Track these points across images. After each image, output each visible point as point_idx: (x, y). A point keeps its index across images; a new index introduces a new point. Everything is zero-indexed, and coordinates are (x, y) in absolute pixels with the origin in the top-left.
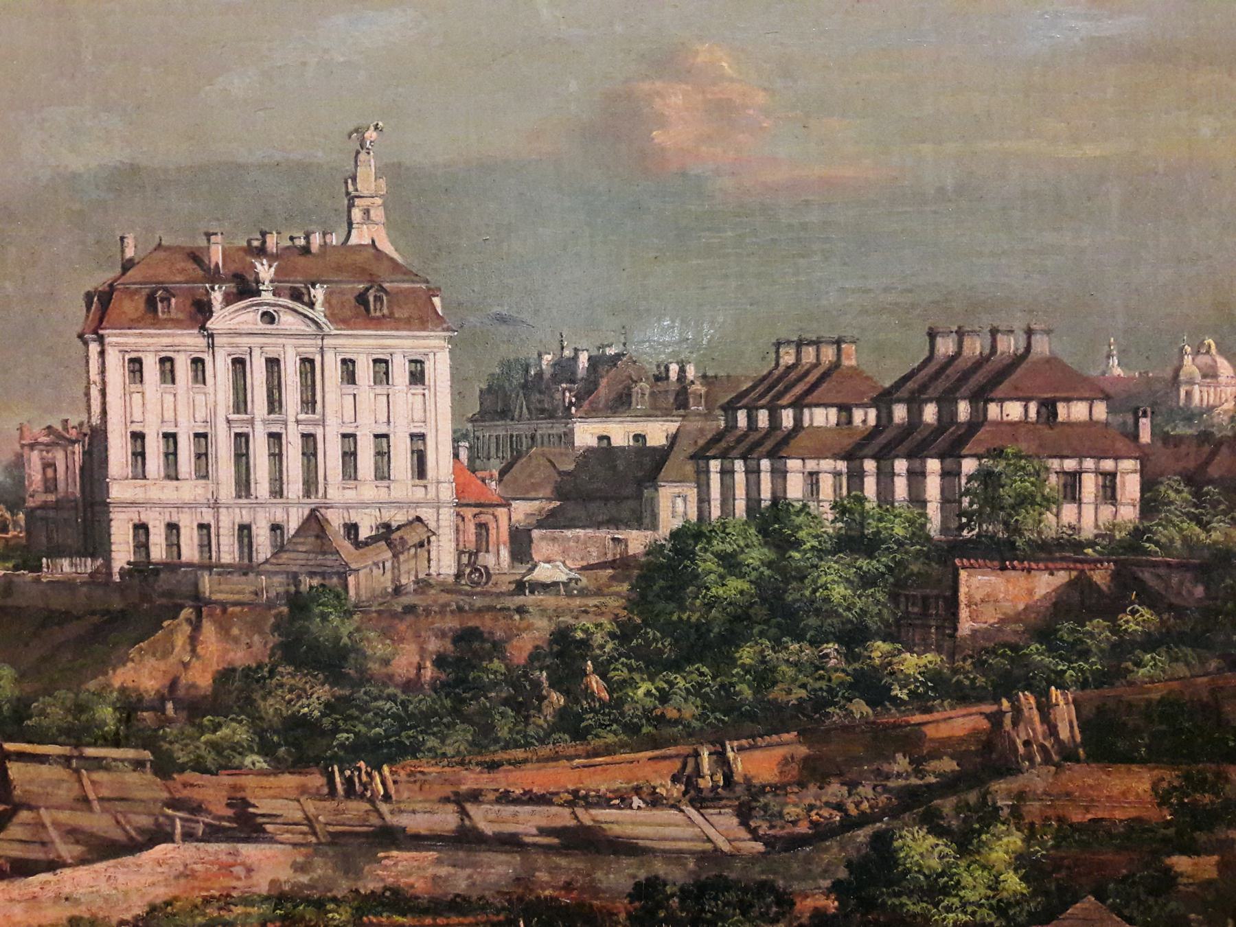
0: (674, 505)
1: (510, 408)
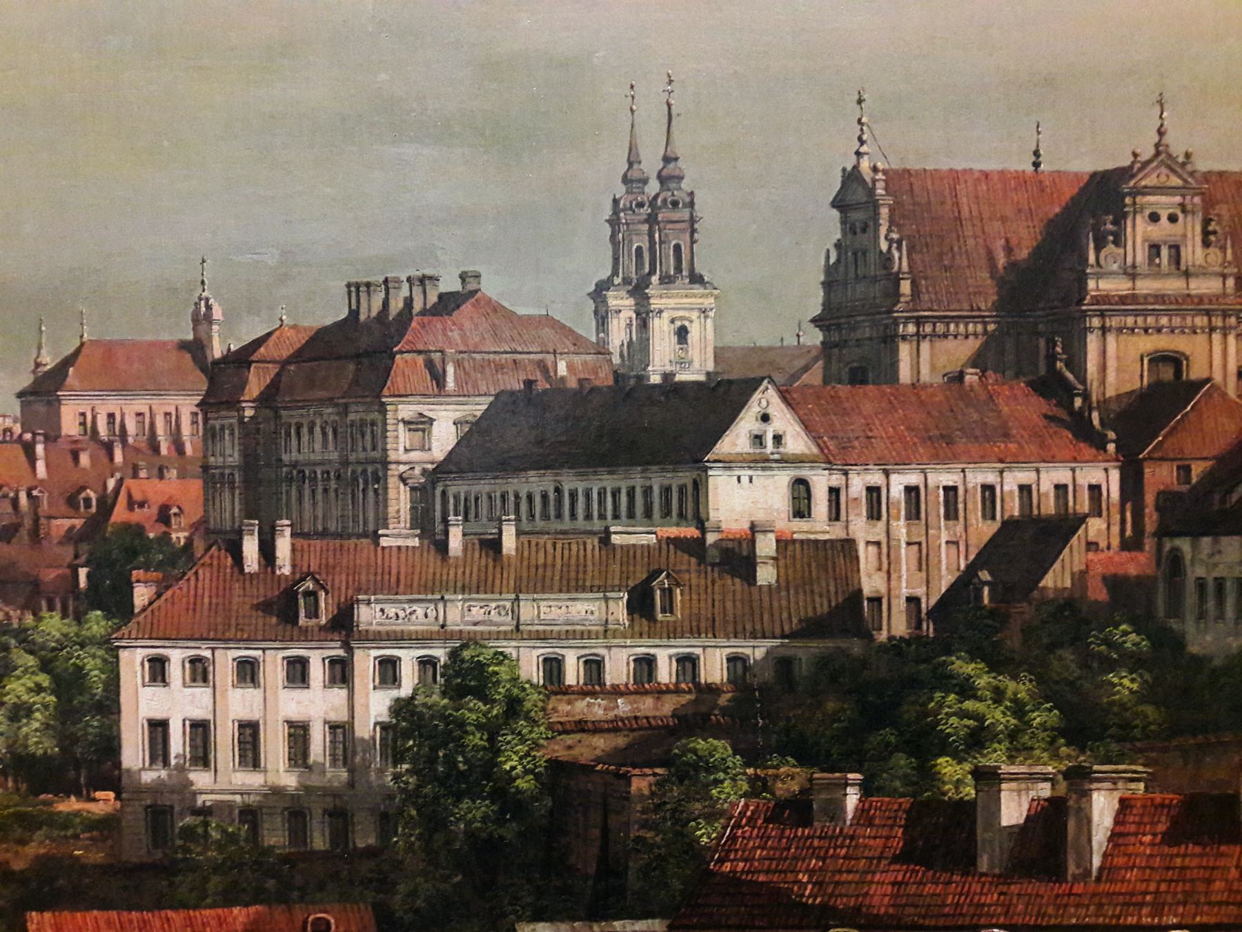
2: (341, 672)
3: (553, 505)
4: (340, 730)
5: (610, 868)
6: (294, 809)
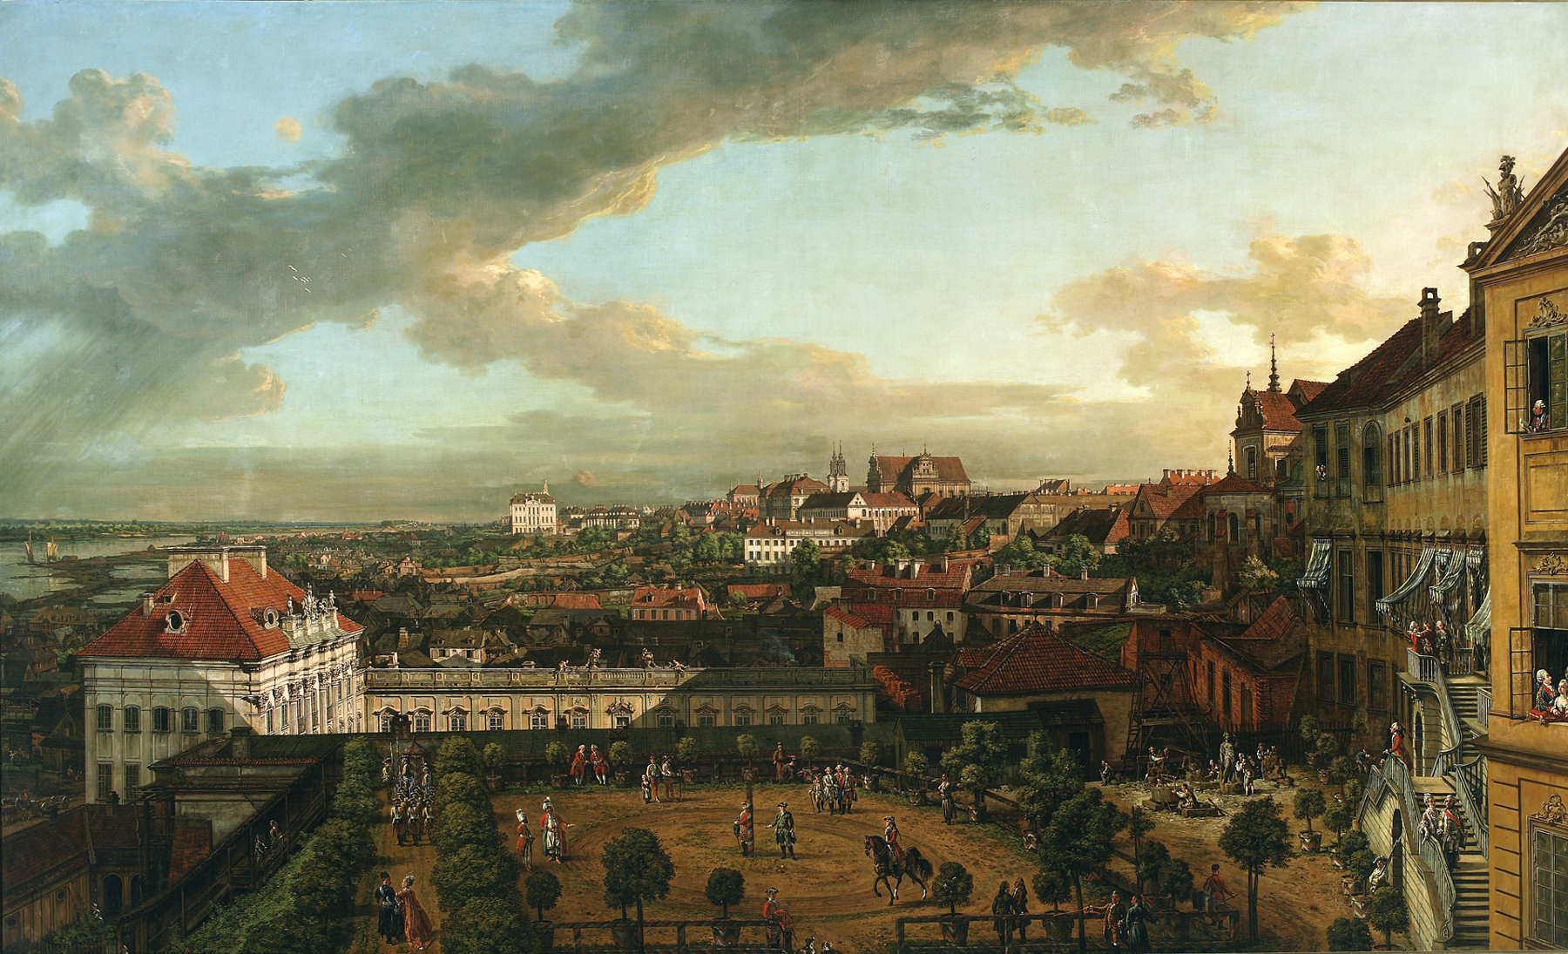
0: (584, 525)
1: (563, 513)
2: (784, 543)
3: (820, 514)
5: (831, 577)
6: (775, 567)
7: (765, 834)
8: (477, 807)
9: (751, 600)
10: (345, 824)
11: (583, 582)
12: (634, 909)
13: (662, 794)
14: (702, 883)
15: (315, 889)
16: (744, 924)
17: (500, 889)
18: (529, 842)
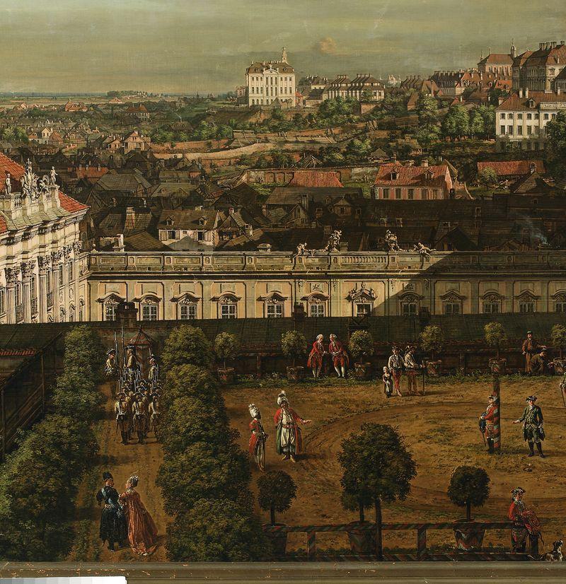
0: (325, 97)
1: (303, 84)
2: (537, 117)
4: (537, 127)
6: (528, 143)
7: (512, 429)
8: (206, 401)
9: (502, 178)
10: (66, 421)
11: (323, 158)
12: (373, 511)
13: (404, 387)
14: (445, 482)
15: (33, 491)
16: (489, 526)
17: (231, 489)
18: (262, 439)
